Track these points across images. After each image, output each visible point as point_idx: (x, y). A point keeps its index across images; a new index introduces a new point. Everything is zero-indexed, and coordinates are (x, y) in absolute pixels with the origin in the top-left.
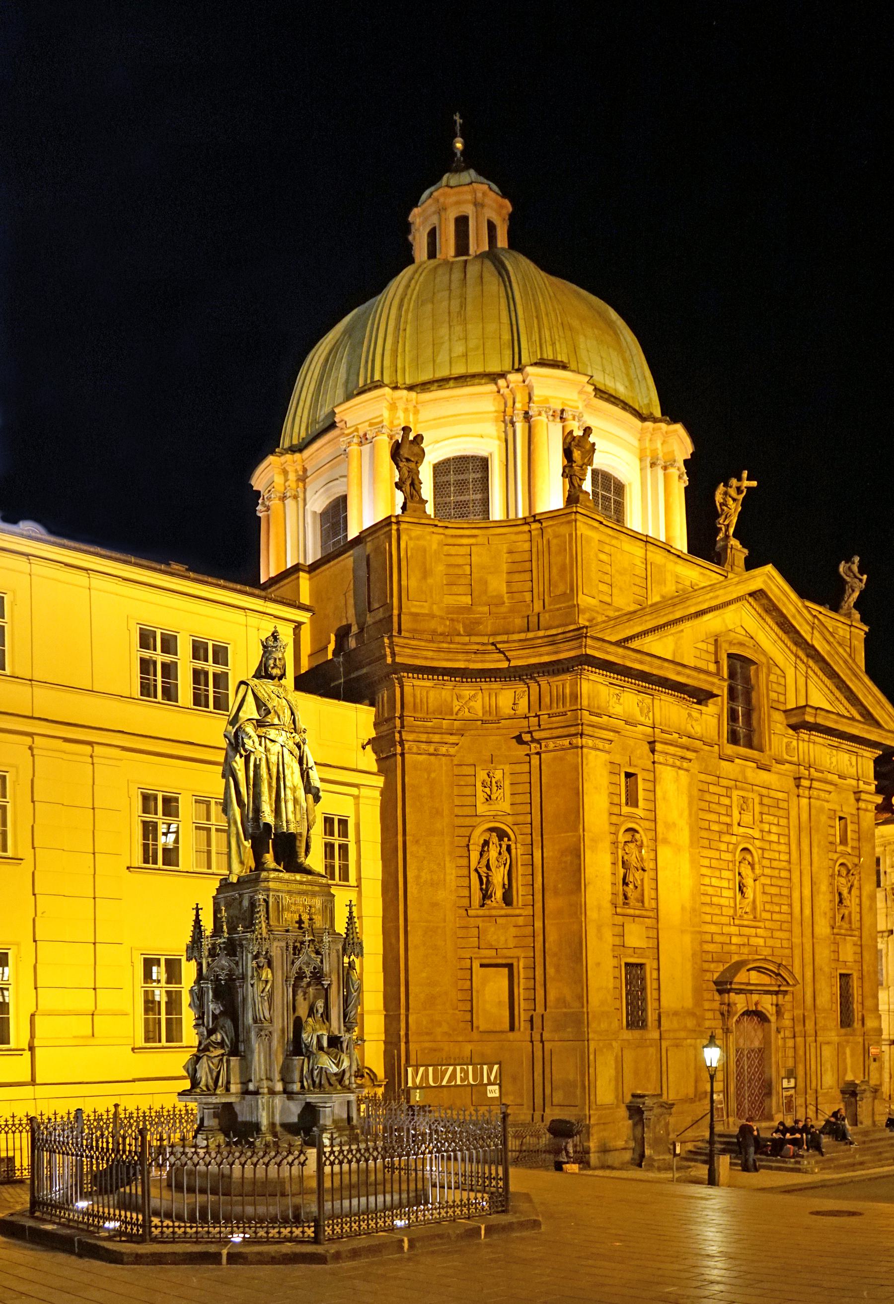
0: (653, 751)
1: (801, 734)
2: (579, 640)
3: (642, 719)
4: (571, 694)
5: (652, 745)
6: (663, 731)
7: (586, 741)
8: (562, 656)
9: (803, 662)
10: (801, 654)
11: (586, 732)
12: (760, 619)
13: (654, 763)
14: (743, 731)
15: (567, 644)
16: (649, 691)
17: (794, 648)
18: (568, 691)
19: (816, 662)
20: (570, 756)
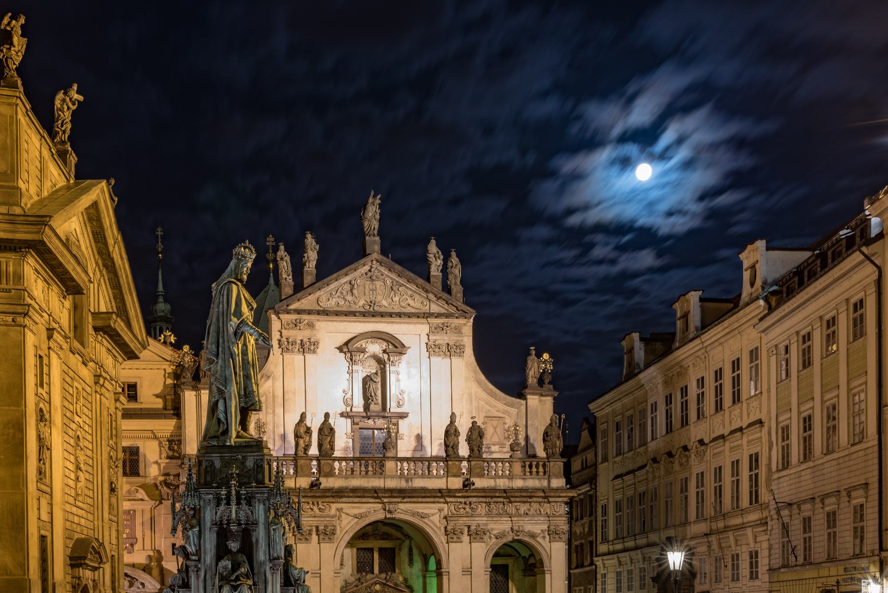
0: (50, 337)
1: (99, 337)
2: (39, 227)
3: (44, 305)
4: (15, 273)
5: (50, 332)
6: (54, 320)
7: (27, 321)
8: (18, 236)
9: (100, 271)
10: (100, 262)
11: (30, 313)
12: (83, 225)
13: (49, 348)
14: (78, 328)
15: (25, 226)
16: (50, 281)
17: (97, 257)
18: (11, 269)
19: (109, 272)
20: (13, 333)
